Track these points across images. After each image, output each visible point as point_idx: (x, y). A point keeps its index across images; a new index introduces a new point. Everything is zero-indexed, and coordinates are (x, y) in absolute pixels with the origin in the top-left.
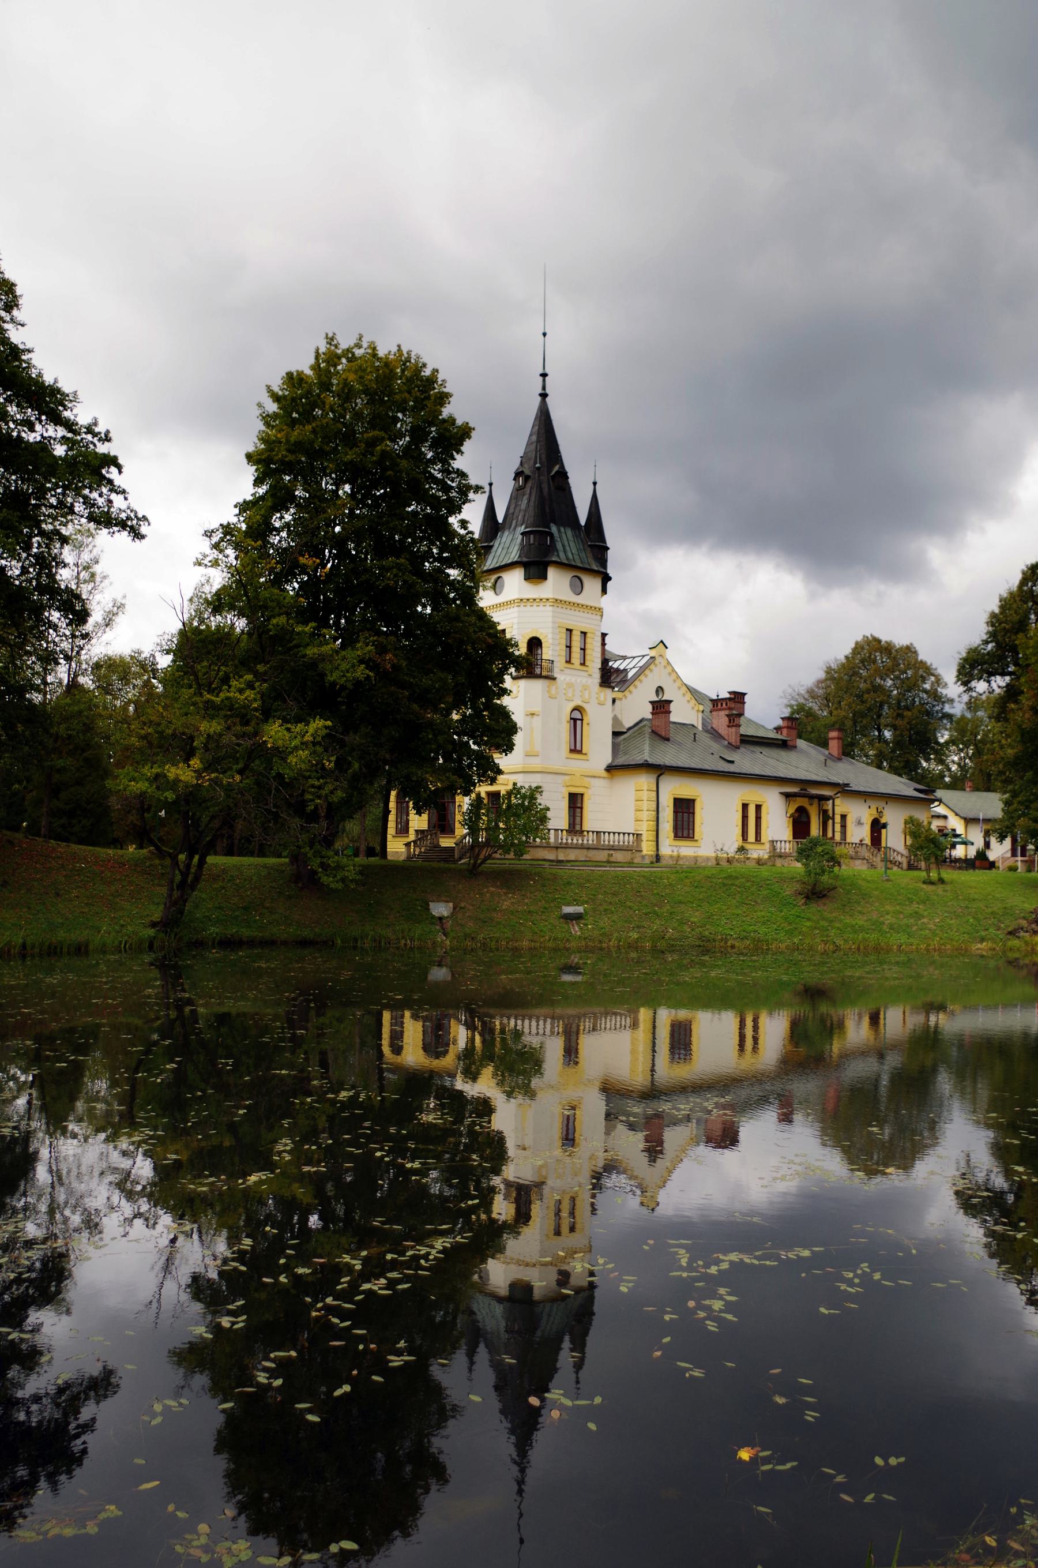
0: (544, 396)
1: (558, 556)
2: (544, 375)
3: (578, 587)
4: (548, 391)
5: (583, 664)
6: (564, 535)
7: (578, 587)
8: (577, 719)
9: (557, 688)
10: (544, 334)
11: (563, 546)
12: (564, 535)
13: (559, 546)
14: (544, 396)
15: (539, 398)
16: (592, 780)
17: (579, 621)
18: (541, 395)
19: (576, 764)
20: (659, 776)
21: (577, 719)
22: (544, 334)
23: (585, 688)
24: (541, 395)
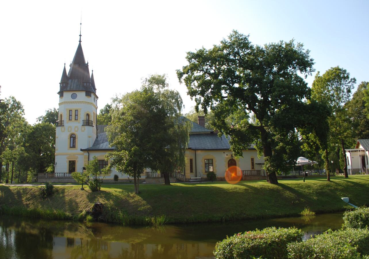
0: (80, 41)
1: (67, 89)
2: (80, 36)
3: (74, 97)
4: (81, 40)
5: (76, 120)
6: (73, 82)
7: (74, 97)
8: (73, 137)
9: (65, 129)
10: (81, 24)
11: (71, 86)
12: (73, 82)
13: (69, 86)
14: (80, 41)
15: (79, 42)
16: (78, 156)
17: (74, 107)
18: (79, 41)
19: (73, 151)
20: (89, 153)
21: (73, 137)
22: (81, 24)
23: (77, 127)
24: (79, 41)
